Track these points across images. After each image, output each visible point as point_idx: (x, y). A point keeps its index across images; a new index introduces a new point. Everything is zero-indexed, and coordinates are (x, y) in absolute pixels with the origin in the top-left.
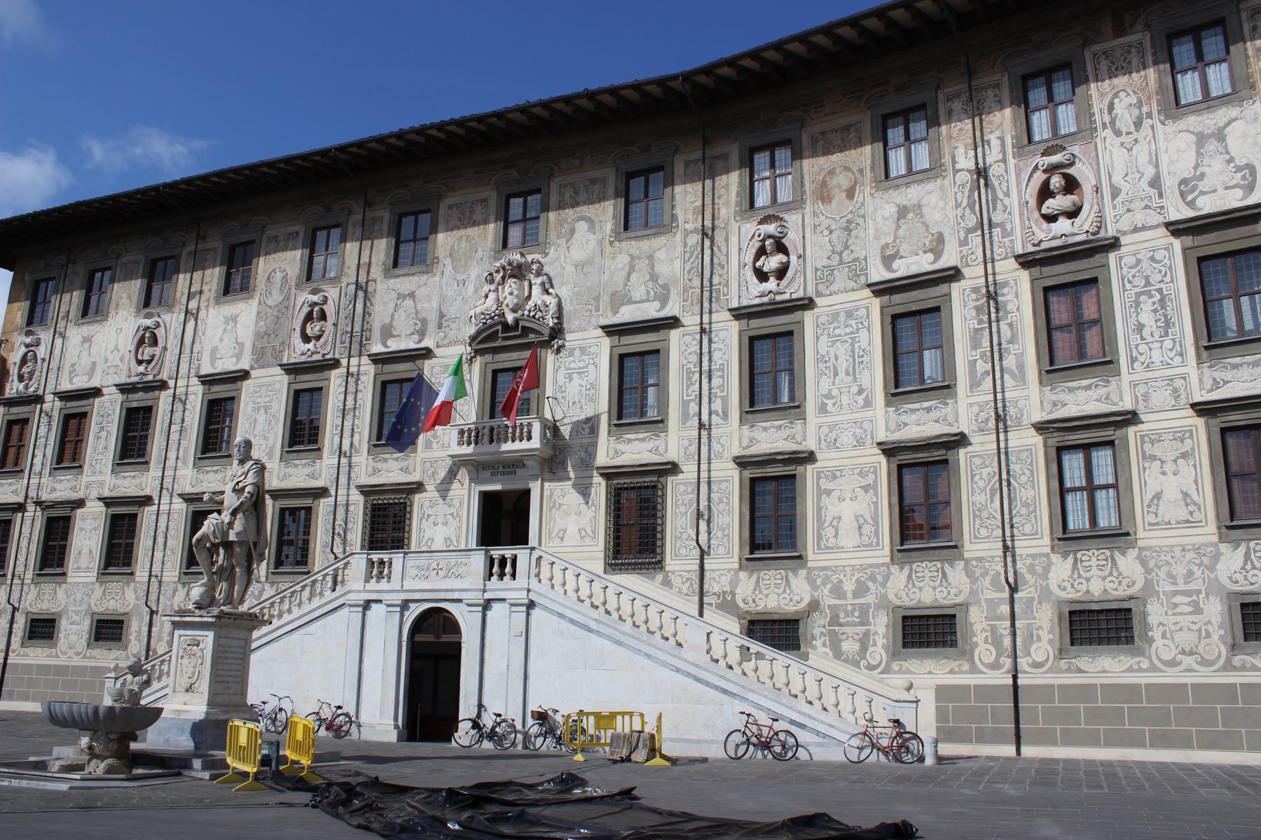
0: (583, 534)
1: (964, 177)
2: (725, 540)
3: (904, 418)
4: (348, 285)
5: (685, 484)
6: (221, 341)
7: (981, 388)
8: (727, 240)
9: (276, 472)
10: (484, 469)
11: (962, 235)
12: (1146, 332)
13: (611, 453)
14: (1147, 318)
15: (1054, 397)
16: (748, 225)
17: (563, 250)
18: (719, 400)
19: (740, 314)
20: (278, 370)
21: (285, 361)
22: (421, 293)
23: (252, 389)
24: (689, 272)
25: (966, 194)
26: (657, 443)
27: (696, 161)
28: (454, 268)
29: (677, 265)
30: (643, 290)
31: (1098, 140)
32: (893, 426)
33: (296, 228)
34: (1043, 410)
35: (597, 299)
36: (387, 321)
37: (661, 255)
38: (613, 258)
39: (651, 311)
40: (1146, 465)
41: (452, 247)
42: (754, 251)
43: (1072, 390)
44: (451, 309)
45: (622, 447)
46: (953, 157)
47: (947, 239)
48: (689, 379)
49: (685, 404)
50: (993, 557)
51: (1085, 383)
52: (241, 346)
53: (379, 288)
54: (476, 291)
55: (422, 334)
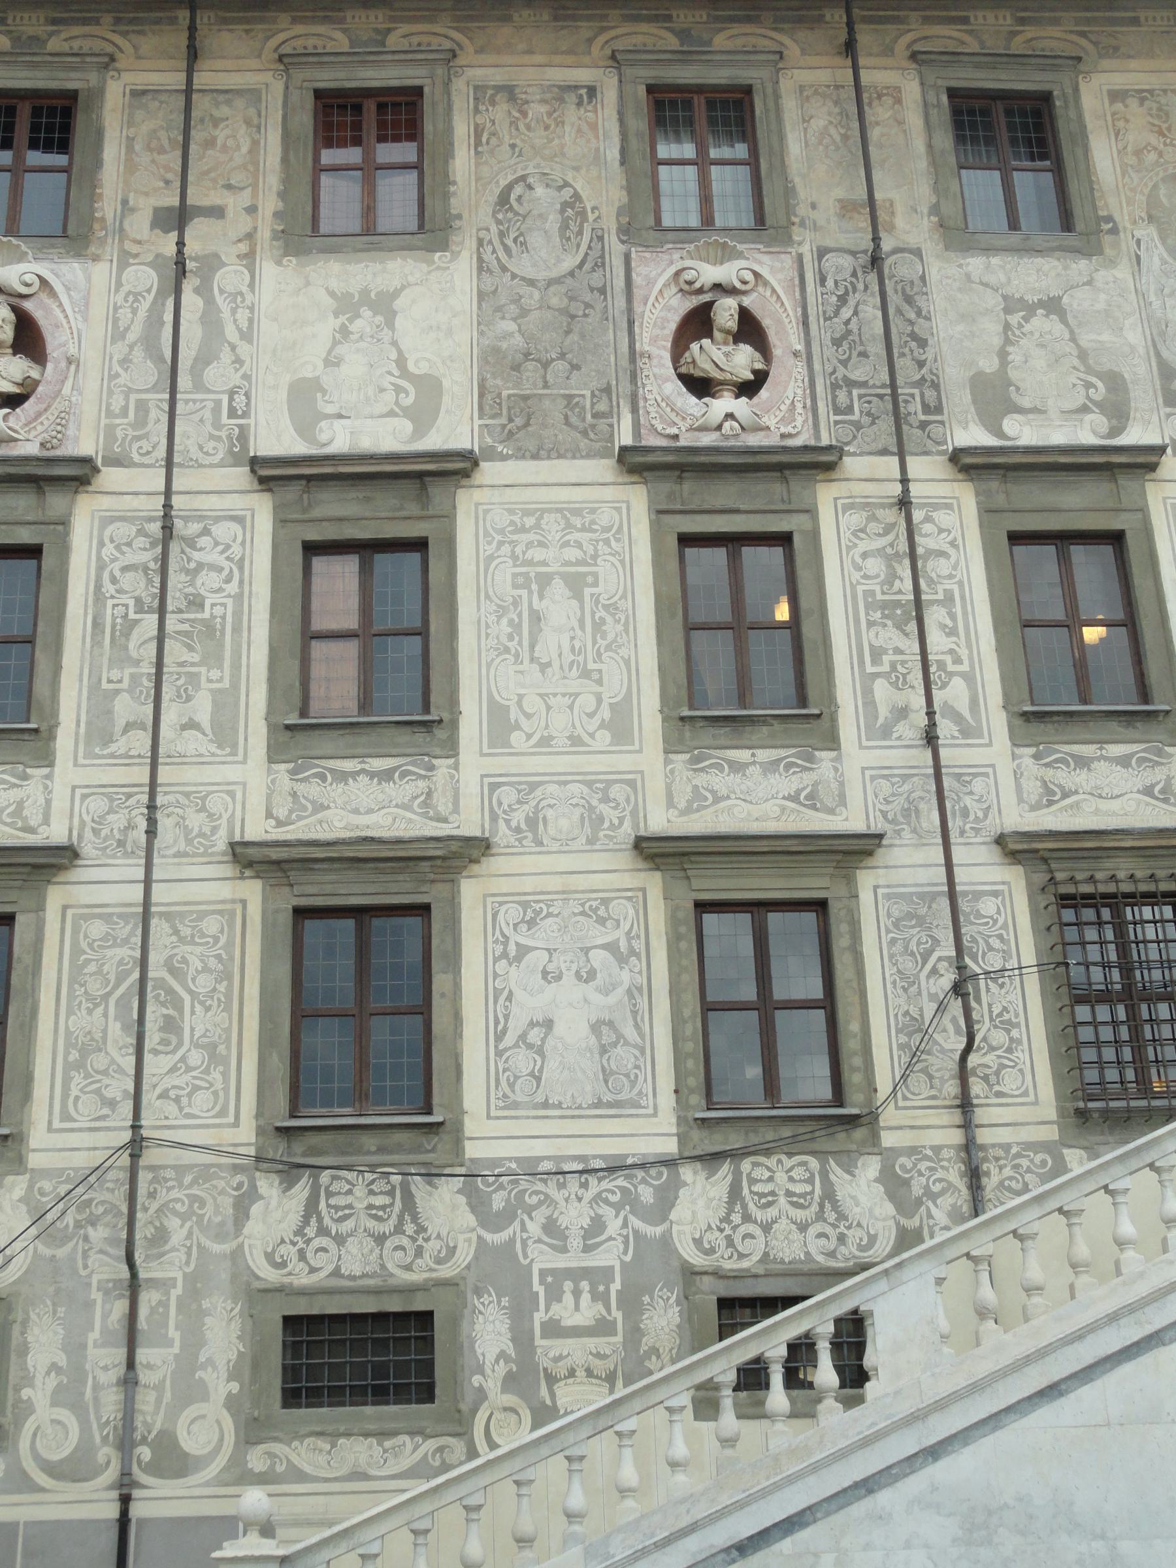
4: (822, 253)
6: (332, 362)
9: (655, 786)
20: (603, 468)
21: (627, 439)
23: (500, 518)
33: (583, 76)
36: (989, 365)
41: (1152, 201)
52: (429, 389)
55: (1119, 414)
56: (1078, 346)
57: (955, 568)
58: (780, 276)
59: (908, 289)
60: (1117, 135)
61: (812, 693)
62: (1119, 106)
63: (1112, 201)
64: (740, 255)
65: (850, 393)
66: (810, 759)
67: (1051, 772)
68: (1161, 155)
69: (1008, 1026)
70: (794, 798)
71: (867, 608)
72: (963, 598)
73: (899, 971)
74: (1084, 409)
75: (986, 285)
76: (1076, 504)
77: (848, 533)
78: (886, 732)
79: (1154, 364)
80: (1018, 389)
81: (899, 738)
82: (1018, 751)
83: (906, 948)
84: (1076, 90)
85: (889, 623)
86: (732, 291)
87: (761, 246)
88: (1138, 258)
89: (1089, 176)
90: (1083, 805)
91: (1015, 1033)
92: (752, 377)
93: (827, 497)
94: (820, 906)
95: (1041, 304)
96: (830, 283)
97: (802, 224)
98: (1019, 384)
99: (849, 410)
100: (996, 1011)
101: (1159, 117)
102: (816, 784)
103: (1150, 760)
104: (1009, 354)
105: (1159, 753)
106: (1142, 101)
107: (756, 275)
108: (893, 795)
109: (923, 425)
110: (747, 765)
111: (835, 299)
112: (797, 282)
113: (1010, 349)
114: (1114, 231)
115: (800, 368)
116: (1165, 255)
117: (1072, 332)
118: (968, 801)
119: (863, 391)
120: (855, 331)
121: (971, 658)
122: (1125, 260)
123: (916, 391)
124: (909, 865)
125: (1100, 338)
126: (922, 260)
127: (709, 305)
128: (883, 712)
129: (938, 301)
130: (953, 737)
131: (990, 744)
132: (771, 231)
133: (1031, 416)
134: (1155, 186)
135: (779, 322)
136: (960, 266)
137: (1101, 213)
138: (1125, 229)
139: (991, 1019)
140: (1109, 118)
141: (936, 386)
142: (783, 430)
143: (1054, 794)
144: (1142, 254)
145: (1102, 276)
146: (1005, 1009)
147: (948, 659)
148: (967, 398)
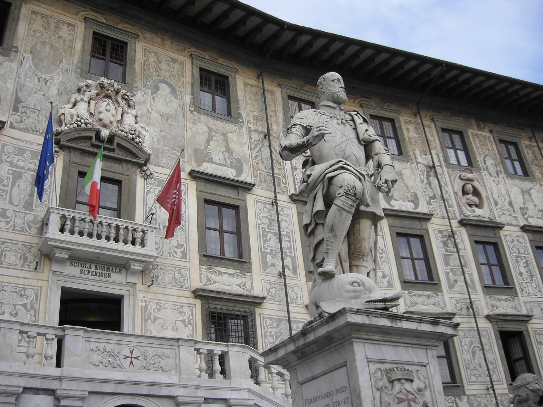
1: (421, 167)
3: (414, 299)
5: (270, 319)
7: (454, 289)
11: (428, 199)
12: (524, 276)
13: (204, 280)
14: (523, 270)
15: (492, 302)
17: (148, 98)
24: (256, 157)
25: (425, 177)
26: (244, 280)
27: (252, 86)
28: (36, 66)
29: (246, 149)
30: (221, 156)
31: (483, 174)
32: (409, 303)
34: (488, 309)
37: (232, 136)
39: (230, 173)
40: (539, 346)
42: (302, 162)
43: (499, 300)
44: (30, 99)
45: (213, 276)
46: (415, 154)
47: (420, 198)
48: (265, 236)
49: (264, 255)
50: (481, 394)
51: (504, 297)
54: (60, 94)
60: (29, 24)
62: (34, 16)
68: (42, 35)
79: (14, 97)
84: (21, 6)
88: (22, 62)
101: (46, 24)
106: (42, 17)
114: (17, 52)
116: (32, 65)
122: (17, 62)
134: (37, 43)
137: (14, 45)
138: (21, 52)
140: (29, 18)
144: (24, 62)
145: (6, 64)
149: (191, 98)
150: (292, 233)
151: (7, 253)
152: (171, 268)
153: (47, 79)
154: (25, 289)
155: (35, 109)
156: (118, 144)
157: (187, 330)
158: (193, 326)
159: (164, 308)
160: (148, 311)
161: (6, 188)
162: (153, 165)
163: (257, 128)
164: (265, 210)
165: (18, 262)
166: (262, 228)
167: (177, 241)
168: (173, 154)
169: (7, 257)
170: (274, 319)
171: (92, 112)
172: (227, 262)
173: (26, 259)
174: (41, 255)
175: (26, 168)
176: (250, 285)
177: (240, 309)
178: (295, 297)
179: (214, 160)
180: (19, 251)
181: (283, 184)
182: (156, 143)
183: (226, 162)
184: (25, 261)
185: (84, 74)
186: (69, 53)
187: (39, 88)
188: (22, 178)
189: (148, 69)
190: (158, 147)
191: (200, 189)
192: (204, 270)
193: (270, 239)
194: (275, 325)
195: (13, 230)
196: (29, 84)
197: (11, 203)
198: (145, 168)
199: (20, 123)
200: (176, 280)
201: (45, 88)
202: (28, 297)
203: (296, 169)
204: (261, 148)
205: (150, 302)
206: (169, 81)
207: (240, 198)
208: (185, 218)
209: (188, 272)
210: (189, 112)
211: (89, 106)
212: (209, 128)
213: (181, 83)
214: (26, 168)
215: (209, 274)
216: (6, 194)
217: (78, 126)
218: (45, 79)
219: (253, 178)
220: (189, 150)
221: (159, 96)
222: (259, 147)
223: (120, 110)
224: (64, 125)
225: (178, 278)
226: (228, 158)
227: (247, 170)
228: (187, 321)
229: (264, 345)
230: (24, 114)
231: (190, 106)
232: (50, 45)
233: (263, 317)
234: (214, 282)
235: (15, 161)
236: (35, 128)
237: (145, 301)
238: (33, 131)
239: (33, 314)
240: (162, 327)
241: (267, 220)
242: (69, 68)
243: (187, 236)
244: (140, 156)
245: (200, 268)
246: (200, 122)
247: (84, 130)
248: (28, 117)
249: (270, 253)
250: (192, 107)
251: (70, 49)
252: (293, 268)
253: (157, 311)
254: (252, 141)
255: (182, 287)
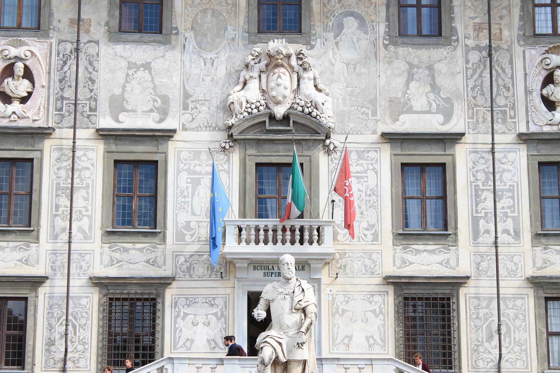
0: (372, 341)
2: (523, 354)
4: (60, 42)
8: (511, 63)
10: (255, 268)
16: (533, 52)
18: (510, 220)
19: (526, 139)
22: (157, 65)
24: (473, 89)
26: (447, 256)
28: (199, 44)
29: (460, 80)
30: (424, 100)
35: (373, 102)
36: (117, 91)
38: (389, 63)
41: (194, 21)
42: (541, 78)
45: (409, 257)
48: (477, 196)
49: (475, 221)
53: (102, 53)
54: (229, 74)
55: (164, 113)
56: (154, 84)
57: (91, 174)
58: (42, 52)
59: (91, 58)
61: (33, 221)
63: (178, 20)
64: (26, 44)
65: (62, 102)
66: (28, 247)
67: (114, 253)
69: (84, 344)
70: (20, 261)
71: (56, 190)
72: (93, 186)
73: (49, 324)
74: (151, 111)
75: (122, 57)
76: (140, 151)
77: (54, 160)
78: (56, 237)
79: (182, 92)
80: (127, 102)
81: (61, 239)
82: (104, 245)
83: (53, 316)
85: (64, 195)
86: (21, 59)
87: (36, 39)
88: (184, 45)
89: (172, 9)
90: (124, 266)
91: (86, 346)
92: (26, 94)
93: (48, 144)
94: (26, 299)
95: (143, 65)
96: (61, 56)
97: (54, 30)
98: (128, 100)
99: (61, 109)
100: (81, 338)
102: (29, 256)
103: (151, 250)
104: (126, 87)
105: (154, 247)
107: (32, 52)
108: (56, 260)
109: (89, 116)
110: (5, 248)
111: (62, 62)
112: (48, 55)
113: (127, 85)
114: (177, 34)
115: (45, 91)
117: (152, 78)
118: (83, 263)
119: (67, 102)
120: (68, 76)
121: (92, 210)
122: (179, 47)
123: (88, 102)
124: (56, 286)
125: (163, 81)
126: (99, 46)
127: (13, 65)
128: (57, 229)
129: (102, 65)
130: (81, 239)
131: (94, 243)
132: (41, 32)
133: (130, 113)
134: (197, 14)
135: (39, 72)
136: (113, 49)
137: (173, 26)
138: (181, 33)
139: (79, 341)
141: (96, 100)
142: (34, 118)
143: (114, 261)
146: (84, 338)
147: (83, 210)
148: (107, 105)
149: (386, 27)
150: (518, 186)
151: (195, 266)
152: (360, 255)
153: (213, 58)
154: (214, 299)
155: (205, 101)
156: (294, 122)
157: (378, 319)
158: (384, 315)
159: (353, 299)
160: (335, 305)
161: (187, 200)
162: (338, 134)
163: (478, 42)
164: (483, 161)
165: (206, 273)
166: (475, 186)
167: (368, 221)
168: (363, 113)
169: (196, 269)
170: (484, 298)
171: (265, 88)
172: (427, 237)
173: (213, 268)
174: (226, 263)
175: (203, 173)
176: (455, 261)
177: (440, 292)
178: (514, 269)
179: (414, 109)
180: (206, 261)
181: (511, 118)
182: (342, 105)
183: (430, 107)
184: (212, 271)
185: (253, 38)
186: (233, 15)
187: (206, 72)
188: (201, 184)
189: (328, 3)
190: (344, 109)
191: (395, 152)
192: (398, 251)
193: (485, 199)
194: (484, 305)
195: (198, 241)
196: (195, 71)
197: (193, 214)
198: (328, 142)
199: (192, 121)
200: (366, 266)
201: (212, 71)
202: (218, 305)
203: (531, 93)
204: (482, 72)
205: (337, 295)
206: (356, 10)
207: (447, 153)
208: (377, 192)
209: (380, 256)
210: (382, 48)
211: (260, 81)
212: (409, 64)
213: (372, 8)
214: (203, 173)
215: (406, 256)
216: (188, 206)
217: (249, 113)
218: (211, 59)
219: (467, 120)
220: (383, 103)
221: (343, 38)
222: (479, 71)
223: (295, 76)
224: (234, 116)
225: (369, 264)
226: (434, 101)
227: (460, 112)
228: (378, 310)
229: (469, 330)
230: (195, 110)
231: (384, 39)
232: (211, 11)
233: (469, 297)
234: (411, 263)
235: (192, 167)
236: (208, 124)
237: (332, 295)
238: (206, 127)
239: (223, 322)
240: (351, 319)
241: (483, 175)
242: (235, 34)
243: (379, 214)
244: (319, 131)
245: (394, 249)
246: (397, 59)
247: (257, 116)
248: (199, 112)
249: (484, 218)
250: (387, 40)
251: (233, 9)
252: (515, 232)
253: (344, 303)
254: (470, 65)
255: (372, 273)
